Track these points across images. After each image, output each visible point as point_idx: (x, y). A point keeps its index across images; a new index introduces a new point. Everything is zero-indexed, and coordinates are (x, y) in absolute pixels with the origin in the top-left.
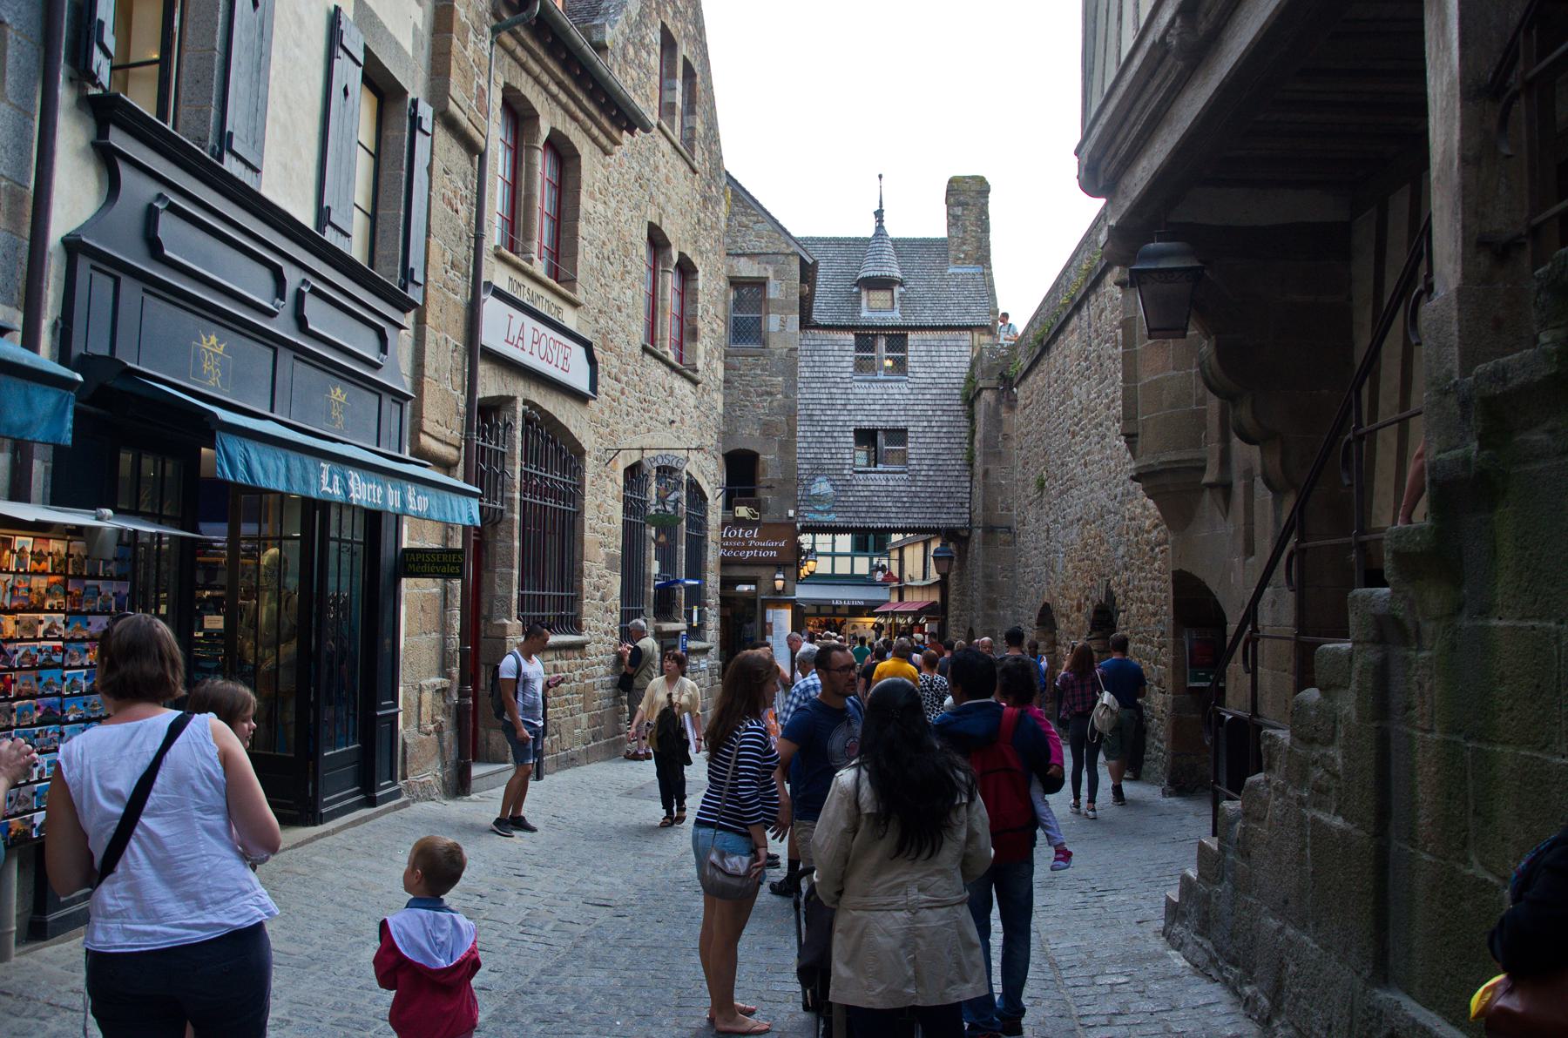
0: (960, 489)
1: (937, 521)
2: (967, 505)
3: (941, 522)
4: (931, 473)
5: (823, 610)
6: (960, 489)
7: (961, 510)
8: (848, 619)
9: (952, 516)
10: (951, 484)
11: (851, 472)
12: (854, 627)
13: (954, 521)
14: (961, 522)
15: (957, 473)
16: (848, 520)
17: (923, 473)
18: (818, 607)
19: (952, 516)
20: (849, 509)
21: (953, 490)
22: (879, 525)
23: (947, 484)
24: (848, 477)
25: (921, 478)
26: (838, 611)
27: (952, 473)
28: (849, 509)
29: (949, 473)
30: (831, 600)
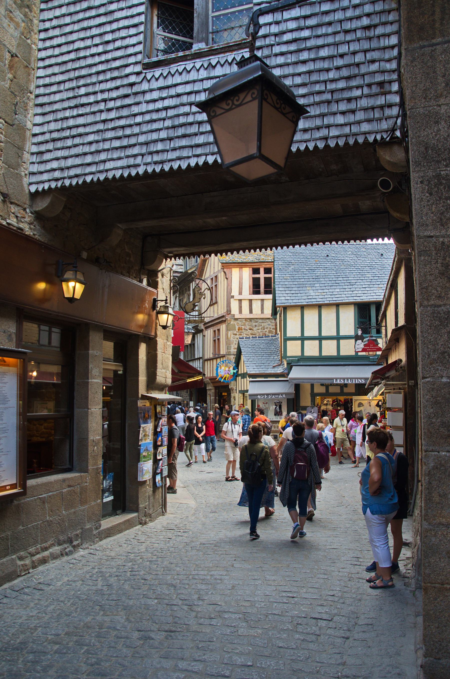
0: (375, 55)
1: (323, 132)
2: (395, 87)
3: (334, 132)
4: (306, 33)
5: (331, 389)
6: (375, 55)
7: (381, 101)
8: (354, 398)
9: (360, 116)
10: (354, 47)
11: (138, 68)
12: (360, 405)
13: (365, 127)
14: (385, 125)
15: (365, 21)
16: (131, 161)
17: (287, 37)
18: (327, 386)
19: (360, 116)
20: (133, 141)
21: (359, 58)
22: (193, 162)
23: (343, 49)
24: (133, 79)
25: (284, 48)
26: (346, 390)
27: (355, 24)
28: (133, 141)
29: (348, 26)
30: (332, 379)
